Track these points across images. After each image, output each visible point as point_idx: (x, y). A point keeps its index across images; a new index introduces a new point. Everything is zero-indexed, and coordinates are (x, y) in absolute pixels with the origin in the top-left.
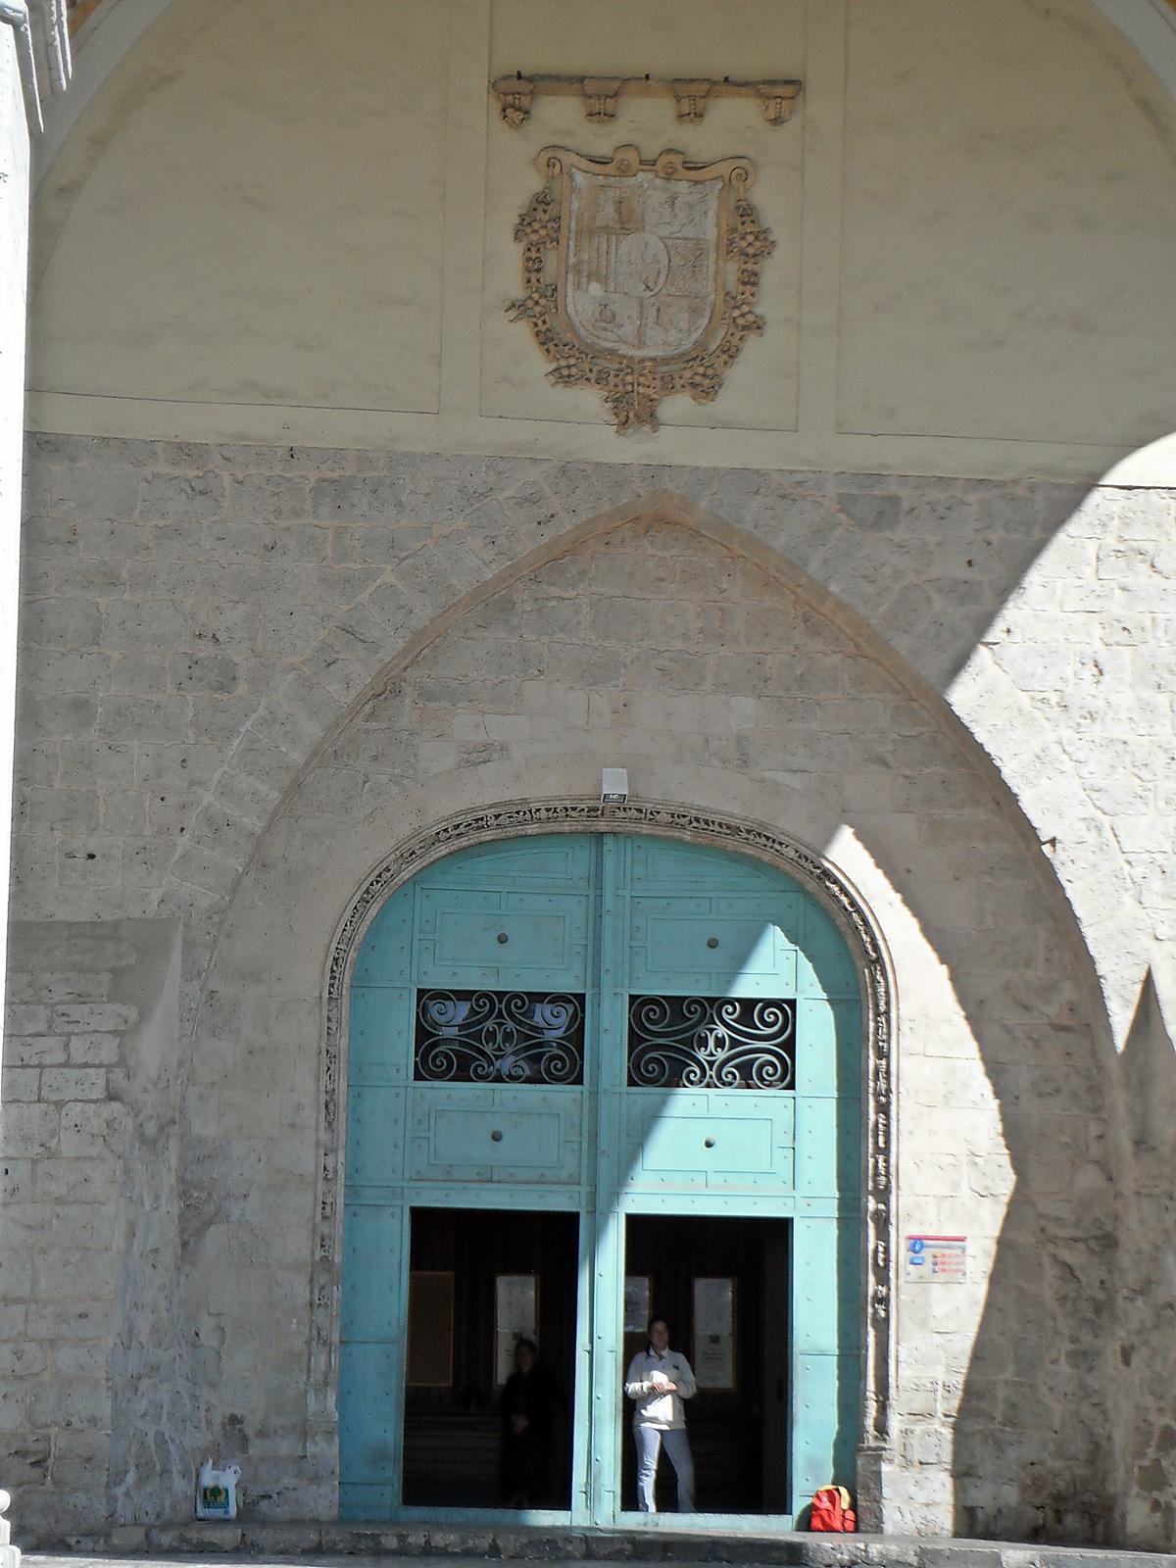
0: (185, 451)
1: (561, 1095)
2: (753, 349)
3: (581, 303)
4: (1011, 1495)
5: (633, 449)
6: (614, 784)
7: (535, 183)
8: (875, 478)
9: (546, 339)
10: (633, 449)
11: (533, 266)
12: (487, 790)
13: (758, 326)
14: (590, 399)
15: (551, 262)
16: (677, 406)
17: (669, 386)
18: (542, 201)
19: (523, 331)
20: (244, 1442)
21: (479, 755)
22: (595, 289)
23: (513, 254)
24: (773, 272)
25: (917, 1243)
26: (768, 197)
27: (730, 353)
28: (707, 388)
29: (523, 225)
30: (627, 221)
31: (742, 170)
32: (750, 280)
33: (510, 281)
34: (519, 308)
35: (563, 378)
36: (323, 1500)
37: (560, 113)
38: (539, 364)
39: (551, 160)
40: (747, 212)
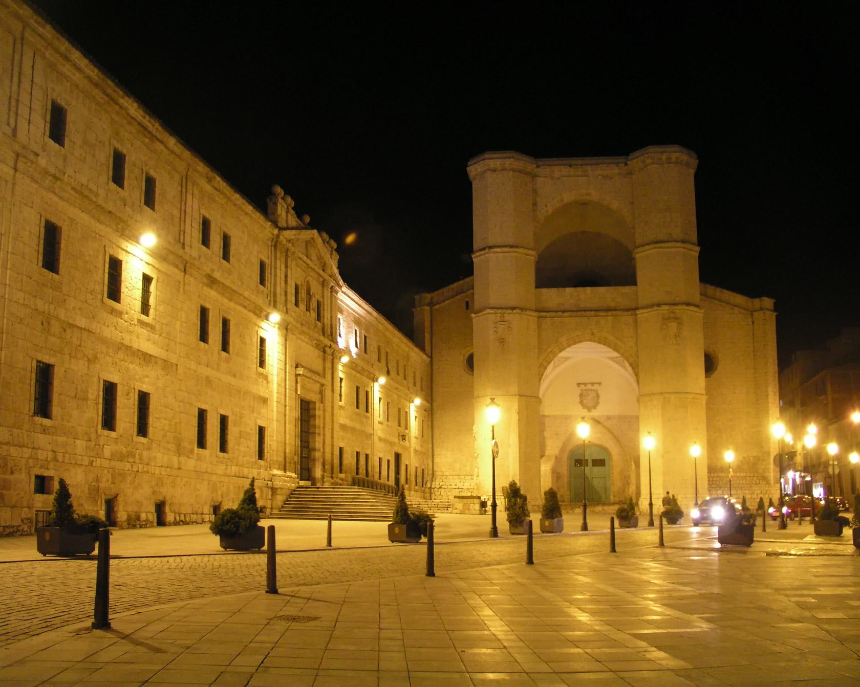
3: (585, 402)
7: (579, 392)
11: (581, 399)
14: (586, 410)
16: (593, 410)
18: (581, 394)
23: (579, 398)
24: (600, 398)
26: (600, 392)
27: (597, 405)
28: (595, 408)
29: (580, 396)
30: (588, 395)
33: (579, 400)
34: (580, 403)
35: (584, 408)
40: (598, 394)
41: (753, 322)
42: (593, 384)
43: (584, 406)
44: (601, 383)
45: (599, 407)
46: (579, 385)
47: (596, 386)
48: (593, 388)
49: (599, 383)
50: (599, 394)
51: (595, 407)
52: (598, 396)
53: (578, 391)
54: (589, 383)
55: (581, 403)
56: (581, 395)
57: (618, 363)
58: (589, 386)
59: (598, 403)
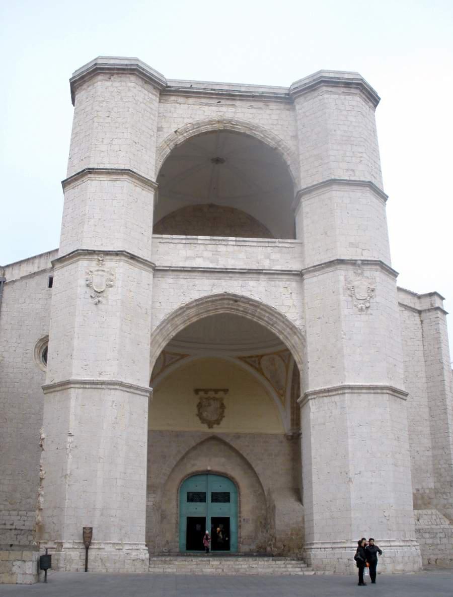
0: (161, 432)
1: (203, 504)
2: (223, 419)
3: (205, 414)
4: (254, 547)
5: (211, 431)
6: (209, 468)
7: (199, 401)
8: (237, 433)
9: (201, 419)
10: (211, 431)
11: (199, 410)
12: (195, 469)
13: (224, 417)
15: (201, 411)
16: (215, 426)
17: (214, 423)
18: (200, 403)
19: (198, 418)
20: (168, 543)
21: (193, 465)
22: (206, 413)
25: (244, 520)
26: (225, 402)
27: (221, 419)
29: (198, 406)
30: (209, 405)
31: (222, 399)
32: (223, 411)
34: (198, 415)
35: (203, 423)
36: (178, 550)
37: (202, 394)
38: (200, 422)
39: (201, 398)
41: (422, 321)
42: (216, 391)
43: (203, 420)
44: (228, 390)
45: (224, 422)
46: (197, 391)
47: (220, 394)
48: (217, 396)
49: (226, 391)
50: (225, 404)
51: (218, 422)
52: (223, 406)
53: (196, 400)
54: (211, 390)
55: (200, 415)
56: (200, 406)
57: (251, 365)
58: (211, 394)
59: (222, 416)
